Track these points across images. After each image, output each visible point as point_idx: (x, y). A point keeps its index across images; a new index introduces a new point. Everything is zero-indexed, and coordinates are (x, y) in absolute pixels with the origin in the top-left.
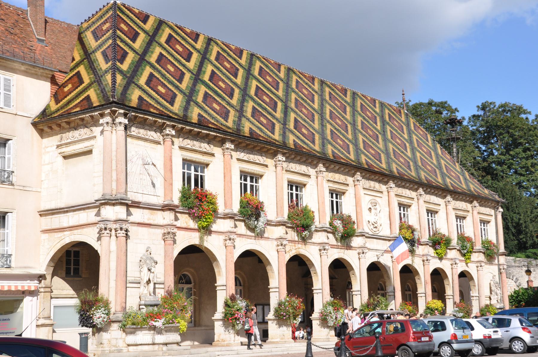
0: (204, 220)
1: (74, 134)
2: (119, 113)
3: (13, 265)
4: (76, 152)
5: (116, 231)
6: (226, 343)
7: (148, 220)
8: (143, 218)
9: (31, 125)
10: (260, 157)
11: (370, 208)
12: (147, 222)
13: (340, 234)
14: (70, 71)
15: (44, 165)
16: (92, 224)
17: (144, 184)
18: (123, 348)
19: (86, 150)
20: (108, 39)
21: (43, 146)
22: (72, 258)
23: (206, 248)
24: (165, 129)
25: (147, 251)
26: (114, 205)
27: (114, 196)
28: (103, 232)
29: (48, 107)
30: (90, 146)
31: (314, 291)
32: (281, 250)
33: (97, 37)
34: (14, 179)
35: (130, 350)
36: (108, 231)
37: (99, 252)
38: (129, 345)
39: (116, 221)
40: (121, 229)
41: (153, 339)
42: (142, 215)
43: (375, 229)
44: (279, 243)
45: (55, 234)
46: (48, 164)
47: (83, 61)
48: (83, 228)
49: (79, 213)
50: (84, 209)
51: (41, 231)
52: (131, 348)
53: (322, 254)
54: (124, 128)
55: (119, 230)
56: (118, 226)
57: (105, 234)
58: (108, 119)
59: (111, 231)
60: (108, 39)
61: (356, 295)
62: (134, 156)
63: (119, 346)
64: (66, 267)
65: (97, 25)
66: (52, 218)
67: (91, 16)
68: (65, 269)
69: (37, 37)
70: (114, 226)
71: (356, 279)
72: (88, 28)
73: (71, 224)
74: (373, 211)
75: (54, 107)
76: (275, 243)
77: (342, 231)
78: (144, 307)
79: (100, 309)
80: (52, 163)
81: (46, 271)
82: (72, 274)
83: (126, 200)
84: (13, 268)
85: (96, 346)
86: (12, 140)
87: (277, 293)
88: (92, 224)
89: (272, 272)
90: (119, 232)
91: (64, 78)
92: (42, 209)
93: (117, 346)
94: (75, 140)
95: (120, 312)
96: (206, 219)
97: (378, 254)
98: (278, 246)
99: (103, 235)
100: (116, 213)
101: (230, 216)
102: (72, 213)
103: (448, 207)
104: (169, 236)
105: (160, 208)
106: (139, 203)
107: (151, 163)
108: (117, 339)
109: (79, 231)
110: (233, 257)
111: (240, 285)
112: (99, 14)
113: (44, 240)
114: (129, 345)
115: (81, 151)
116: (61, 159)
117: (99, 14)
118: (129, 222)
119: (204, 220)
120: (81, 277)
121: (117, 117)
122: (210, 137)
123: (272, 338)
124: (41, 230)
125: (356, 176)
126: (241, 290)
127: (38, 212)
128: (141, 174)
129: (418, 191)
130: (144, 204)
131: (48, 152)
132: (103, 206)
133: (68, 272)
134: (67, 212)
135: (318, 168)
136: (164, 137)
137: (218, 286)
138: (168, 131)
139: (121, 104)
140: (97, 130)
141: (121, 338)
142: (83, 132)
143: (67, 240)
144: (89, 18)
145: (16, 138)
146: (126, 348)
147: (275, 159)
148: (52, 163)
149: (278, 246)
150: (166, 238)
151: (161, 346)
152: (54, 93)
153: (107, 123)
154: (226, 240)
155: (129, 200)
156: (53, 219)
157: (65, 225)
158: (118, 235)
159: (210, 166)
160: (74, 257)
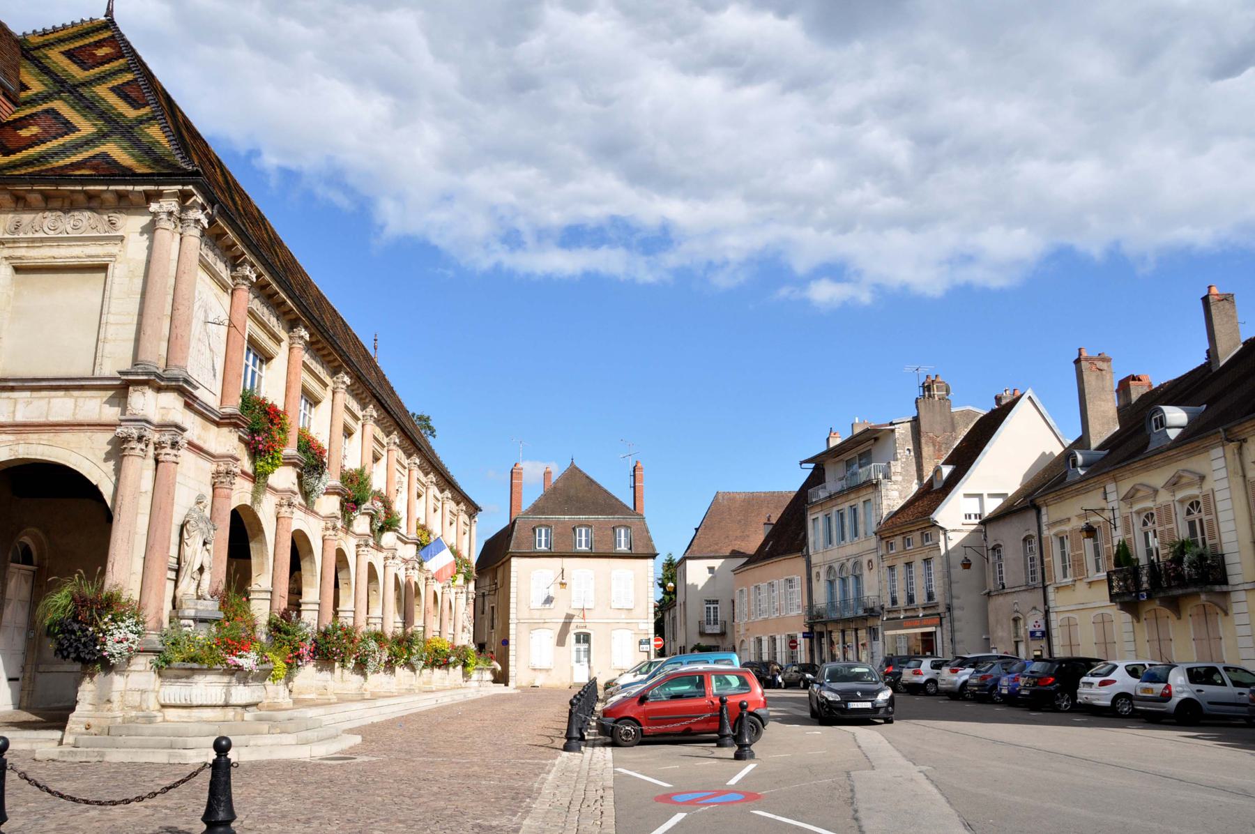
0: (270, 461)
1: (59, 224)
2: (195, 201)
4: (59, 262)
5: (156, 449)
7: (198, 439)
10: (321, 369)
13: (380, 524)
16: (88, 425)
18: (155, 713)
23: (1207, 449)
24: (241, 265)
25: (198, 503)
26: (159, 389)
28: (133, 444)
30: (104, 256)
32: (331, 537)
35: (167, 718)
36: (143, 446)
38: (163, 706)
39: (162, 427)
41: (228, 694)
44: (330, 525)
48: (62, 431)
49: (50, 398)
50: (66, 388)
52: (171, 714)
53: (360, 553)
55: (169, 446)
56: (167, 438)
57: (137, 452)
58: (172, 205)
63: (148, 708)
70: (155, 437)
73: (20, 418)
76: (323, 524)
77: (383, 519)
78: (191, 622)
79: (123, 621)
85: (90, 707)
87: (317, 613)
88: (88, 425)
89: (313, 576)
91: (7, 115)
93: (144, 707)
94: (60, 235)
95: (154, 630)
96: (272, 458)
98: (327, 529)
99: (132, 452)
101: (296, 461)
102: (28, 394)
104: (228, 479)
108: (143, 692)
109: (45, 436)
112: (56, 35)
114: (163, 706)
116: (9, 271)
117: (56, 35)
119: (270, 461)
121: (190, 208)
122: (283, 309)
123: (300, 693)
125: (391, 436)
129: (429, 476)
132: (140, 388)
134: (12, 389)
135: (368, 410)
136: (238, 281)
138: (247, 270)
140: (131, 224)
141: (153, 691)
142: (85, 221)
146: (159, 714)
147: (335, 379)
149: (327, 529)
150: (222, 482)
151: (239, 709)
153: (170, 214)
154: (281, 506)
158: (162, 458)
159: (274, 360)
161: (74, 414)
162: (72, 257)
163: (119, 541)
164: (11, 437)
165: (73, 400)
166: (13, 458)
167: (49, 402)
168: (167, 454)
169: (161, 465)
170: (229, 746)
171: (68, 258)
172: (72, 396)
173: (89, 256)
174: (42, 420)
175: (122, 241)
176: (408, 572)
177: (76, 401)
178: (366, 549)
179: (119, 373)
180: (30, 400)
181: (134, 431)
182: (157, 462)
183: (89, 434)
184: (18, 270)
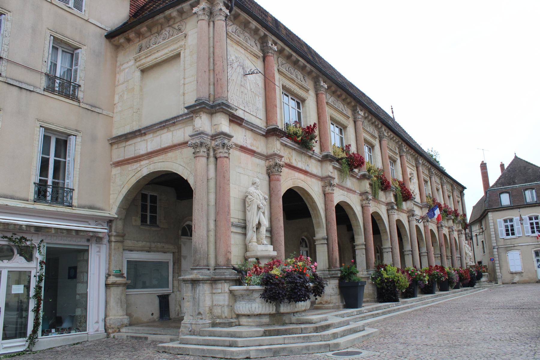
3: (75, 202)
4: (159, 60)
8: (245, 142)
9: (105, 39)
12: (249, 147)
17: (245, 99)
19: (171, 54)
21: (118, 64)
22: (149, 204)
32: (366, 205)
34: (80, 95)
37: (191, 182)
42: (245, 138)
45: (129, 165)
48: (166, 153)
51: (111, 165)
53: (390, 213)
59: (208, 150)
62: (234, 61)
64: (142, 214)
66: (125, 147)
68: (139, 215)
73: (150, 150)
82: (148, 222)
84: (75, 207)
86: (81, 48)
103: (443, 187)
106: (242, 120)
111: (306, 247)
113: (115, 175)
115: (165, 57)
120: (158, 226)
126: (307, 252)
133: (144, 220)
137: (316, 240)
143: (145, 172)
145: (85, 47)
152: (133, 14)
157: (142, 152)
158: (218, 155)
160: (147, 215)
163: (196, 211)
164: (147, 162)
166: (149, 173)
167: (161, 137)
168: (222, 152)
169: (218, 160)
171: (162, 56)
172: (170, 131)
174: (159, 148)
175: (185, 37)
176: (425, 224)
177: (172, 133)
179: (187, 108)
180: (152, 138)
182: (216, 159)
183: (180, 150)
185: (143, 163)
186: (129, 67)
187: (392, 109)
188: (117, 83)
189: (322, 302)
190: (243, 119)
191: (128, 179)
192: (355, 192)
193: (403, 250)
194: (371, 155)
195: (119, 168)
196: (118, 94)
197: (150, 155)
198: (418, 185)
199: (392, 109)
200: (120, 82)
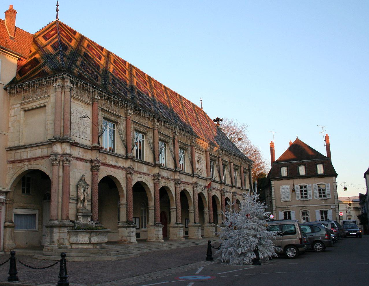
4: (34, 107)
6: (127, 242)
7: (82, 156)
9: (4, 90)
11: (198, 160)
12: (82, 157)
14: (29, 58)
15: (11, 117)
18: (68, 246)
20: (55, 38)
21: (11, 104)
27: (62, 137)
29: (15, 78)
31: (171, 209)
33: (47, 38)
35: (73, 247)
37: (50, 177)
40: (67, 160)
41: (90, 240)
43: (200, 174)
46: (14, 116)
47: (38, 51)
48: (39, 160)
50: (39, 146)
51: (7, 162)
52: (74, 246)
53: (176, 186)
54: (70, 90)
56: (64, 158)
59: (60, 162)
60: (55, 38)
61: (191, 213)
63: (65, 244)
65: (45, 33)
67: (41, 29)
68: (21, 189)
69: (10, 35)
71: (191, 203)
72: (39, 35)
73: (29, 157)
74: (200, 162)
75: (19, 78)
78: (81, 217)
80: (16, 115)
81: (10, 189)
82: (26, 193)
83: (71, 140)
85: (49, 244)
90: (66, 162)
92: (8, 147)
93: (64, 244)
97: (202, 188)
100: (63, 149)
105: (90, 149)
106: (78, 143)
107: (86, 116)
108: (64, 239)
109: (35, 162)
110: (132, 185)
113: (9, 168)
116: (22, 113)
118: (72, 156)
124: (7, 161)
127: (6, 148)
128: (79, 124)
130: (81, 145)
131: (14, 108)
133: (23, 192)
139: (70, 71)
141: (67, 239)
143: (26, 168)
144: (42, 28)
146: (70, 246)
148: (16, 115)
155: (73, 141)
156: (16, 154)
157: (25, 158)
158: (64, 165)
161: (41, 154)
162: (37, 105)
163: (53, 192)
164: (27, 163)
165: (41, 150)
168: (66, 164)
169: (64, 167)
170: (65, 255)
171: (36, 105)
172: (40, 149)
173: (41, 104)
175: (49, 97)
177: (41, 150)
178: (178, 185)
181: (54, 158)
182: (63, 166)
184: (25, 111)
185: (25, 163)
186: (17, 107)
187: (201, 100)
188: (10, 115)
189: (122, 240)
190: (78, 143)
191: (16, 171)
192: (150, 175)
193: (188, 210)
194: (166, 148)
195: (11, 164)
196: (11, 122)
197: (29, 160)
198: (206, 164)
199: (201, 100)
200: (12, 115)
